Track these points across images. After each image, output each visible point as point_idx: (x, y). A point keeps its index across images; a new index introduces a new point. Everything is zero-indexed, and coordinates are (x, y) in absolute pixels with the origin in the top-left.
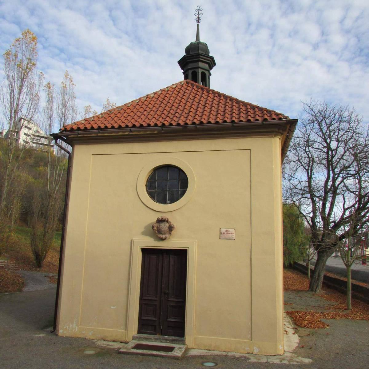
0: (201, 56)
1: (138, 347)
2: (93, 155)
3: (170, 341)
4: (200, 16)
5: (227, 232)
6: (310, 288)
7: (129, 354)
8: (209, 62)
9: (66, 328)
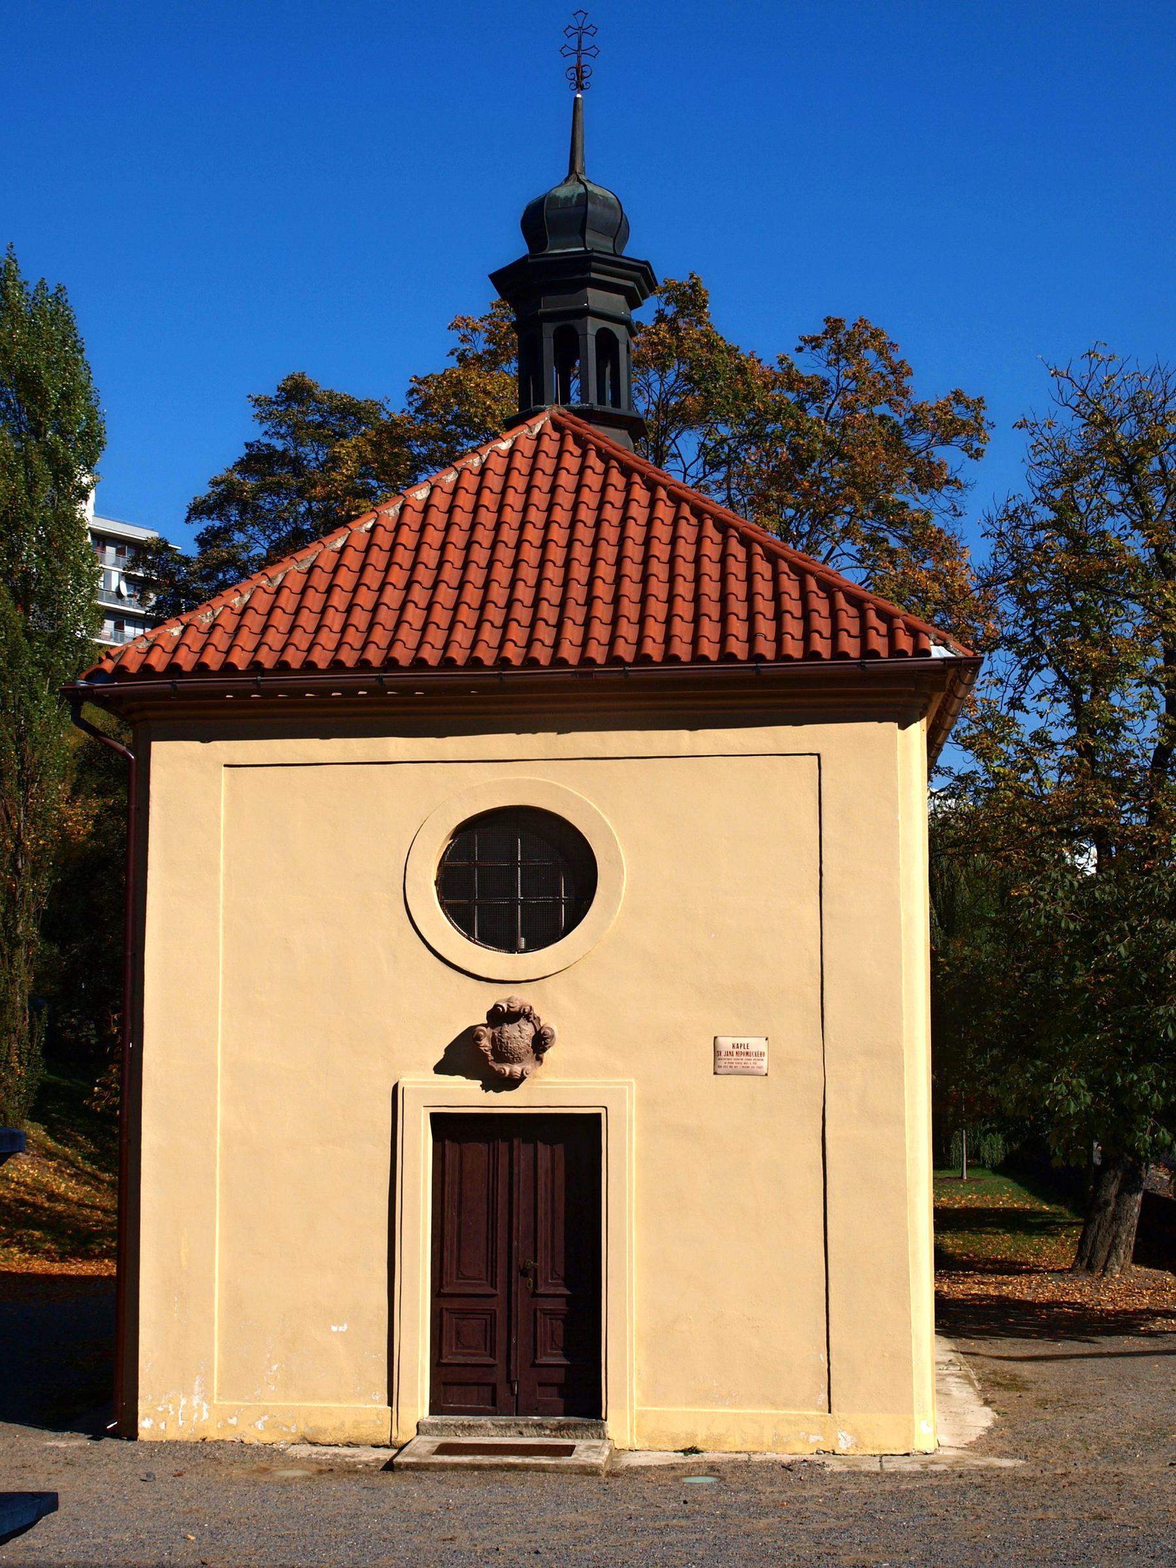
1: (444, 1449)
2: (225, 766)
3: (551, 1430)
4: (585, 60)
5: (739, 1050)
6: (1080, 1256)
7: (428, 1469)
8: (630, 284)
9: (167, 1411)
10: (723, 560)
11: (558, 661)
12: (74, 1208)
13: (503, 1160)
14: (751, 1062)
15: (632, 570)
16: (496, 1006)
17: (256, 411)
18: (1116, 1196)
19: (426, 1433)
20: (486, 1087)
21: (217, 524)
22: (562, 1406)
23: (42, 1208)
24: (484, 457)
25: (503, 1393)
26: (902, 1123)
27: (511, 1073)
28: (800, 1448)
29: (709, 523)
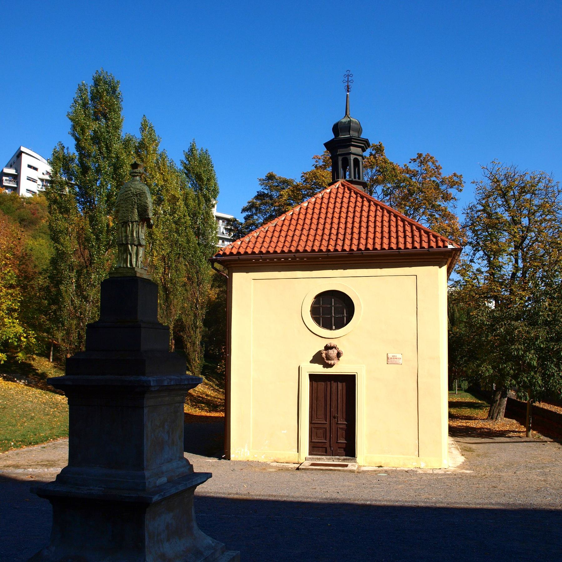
0: (353, 140)
1: (313, 465)
6: (489, 415)
8: (363, 145)
10: (389, 222)
11: (343, 250)
12: (213, 399)
14: (397, 361)
16: (327, 345)
17: (260, 182)
18: (500, 399)
19: (308, 460)
20: (324, 367)
21: (250, 213)
22: (345, 454)
23: (204, 398)
24: (323, 194)
25: (328, 449)
27: (331, 363)
28: (410, 465)
29: (385, 211)
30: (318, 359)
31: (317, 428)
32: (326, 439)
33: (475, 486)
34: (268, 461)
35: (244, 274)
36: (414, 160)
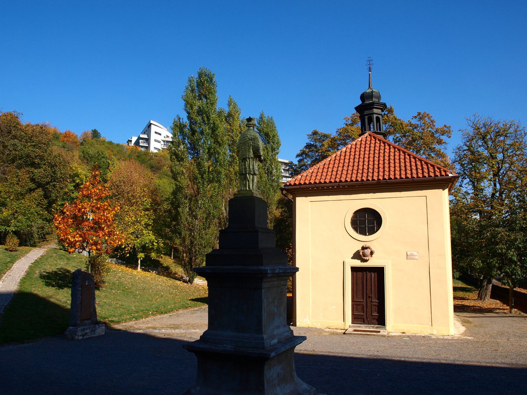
1: (355, 331)
4: (371, 66)
6: (478, 297)
8: (382, 107)
9: (302, 321)
10: (405, 159)
11: (373, 180)
13: (365, 276)
14: (414, 257)
15: (387, 162)
17: (308, 137)
18: (486, 285)
21: (301, 158)
25: (365, 320)
26: (446, 269)
29: (401, 152)
30: (357, 256)
31: (357, 305)
32: (363, 313)
33: (480, 349)
34: (323, 327)
35: (304, 198)
36: (416, 117)
